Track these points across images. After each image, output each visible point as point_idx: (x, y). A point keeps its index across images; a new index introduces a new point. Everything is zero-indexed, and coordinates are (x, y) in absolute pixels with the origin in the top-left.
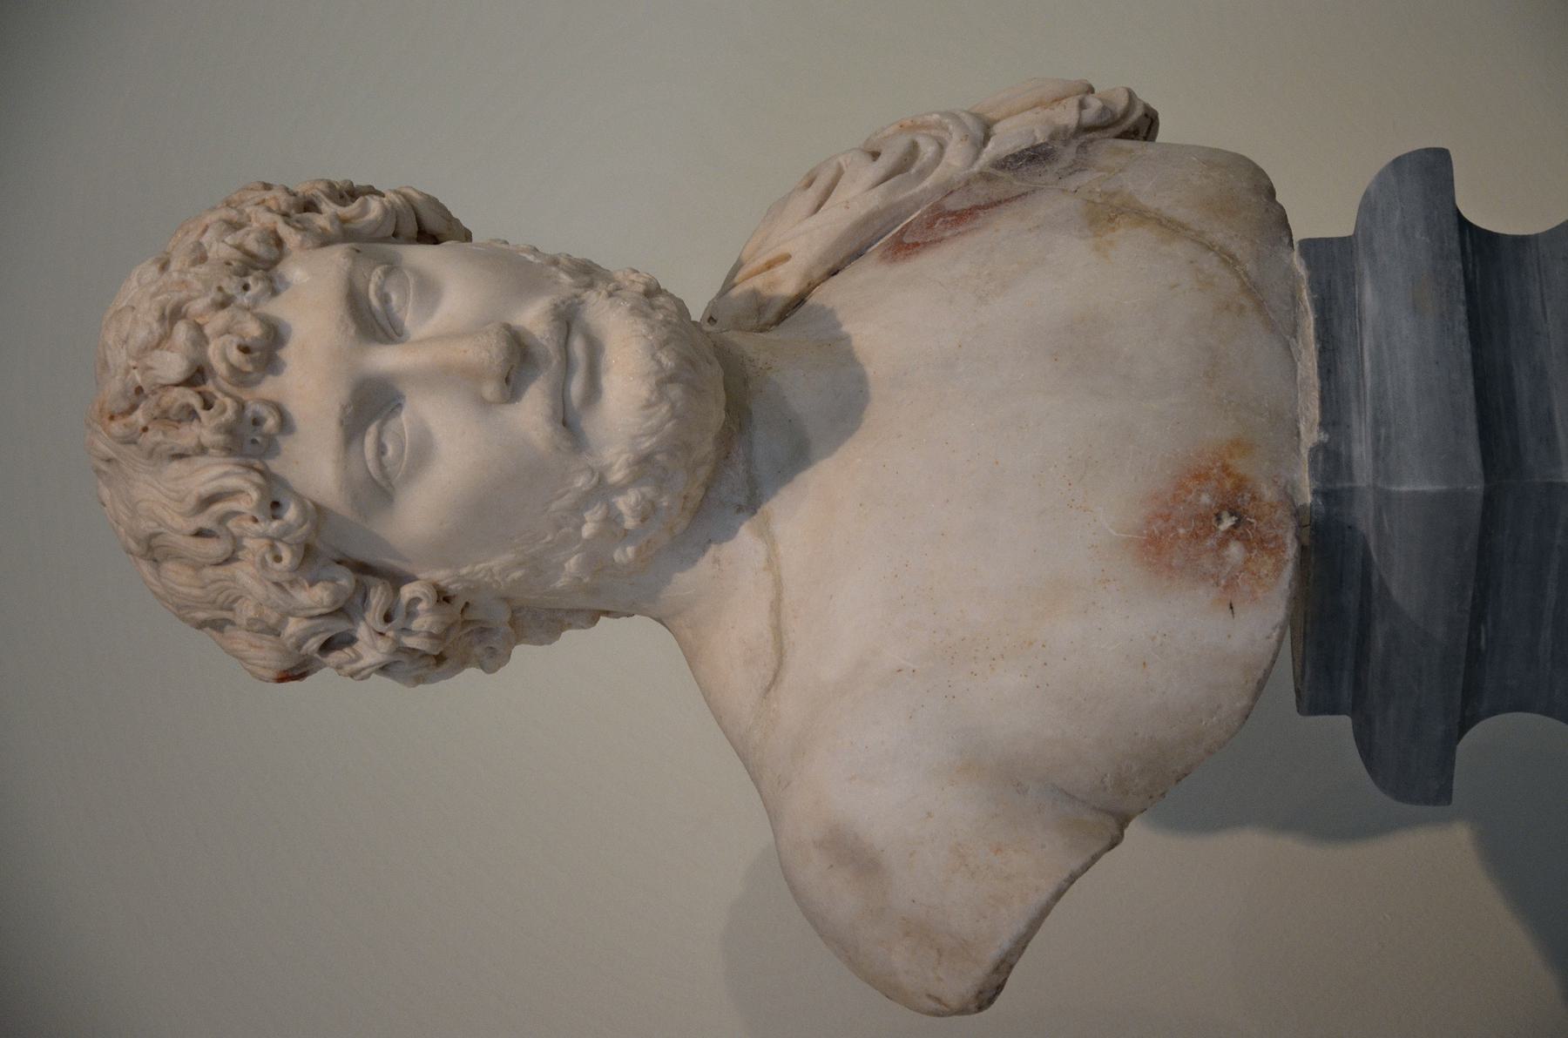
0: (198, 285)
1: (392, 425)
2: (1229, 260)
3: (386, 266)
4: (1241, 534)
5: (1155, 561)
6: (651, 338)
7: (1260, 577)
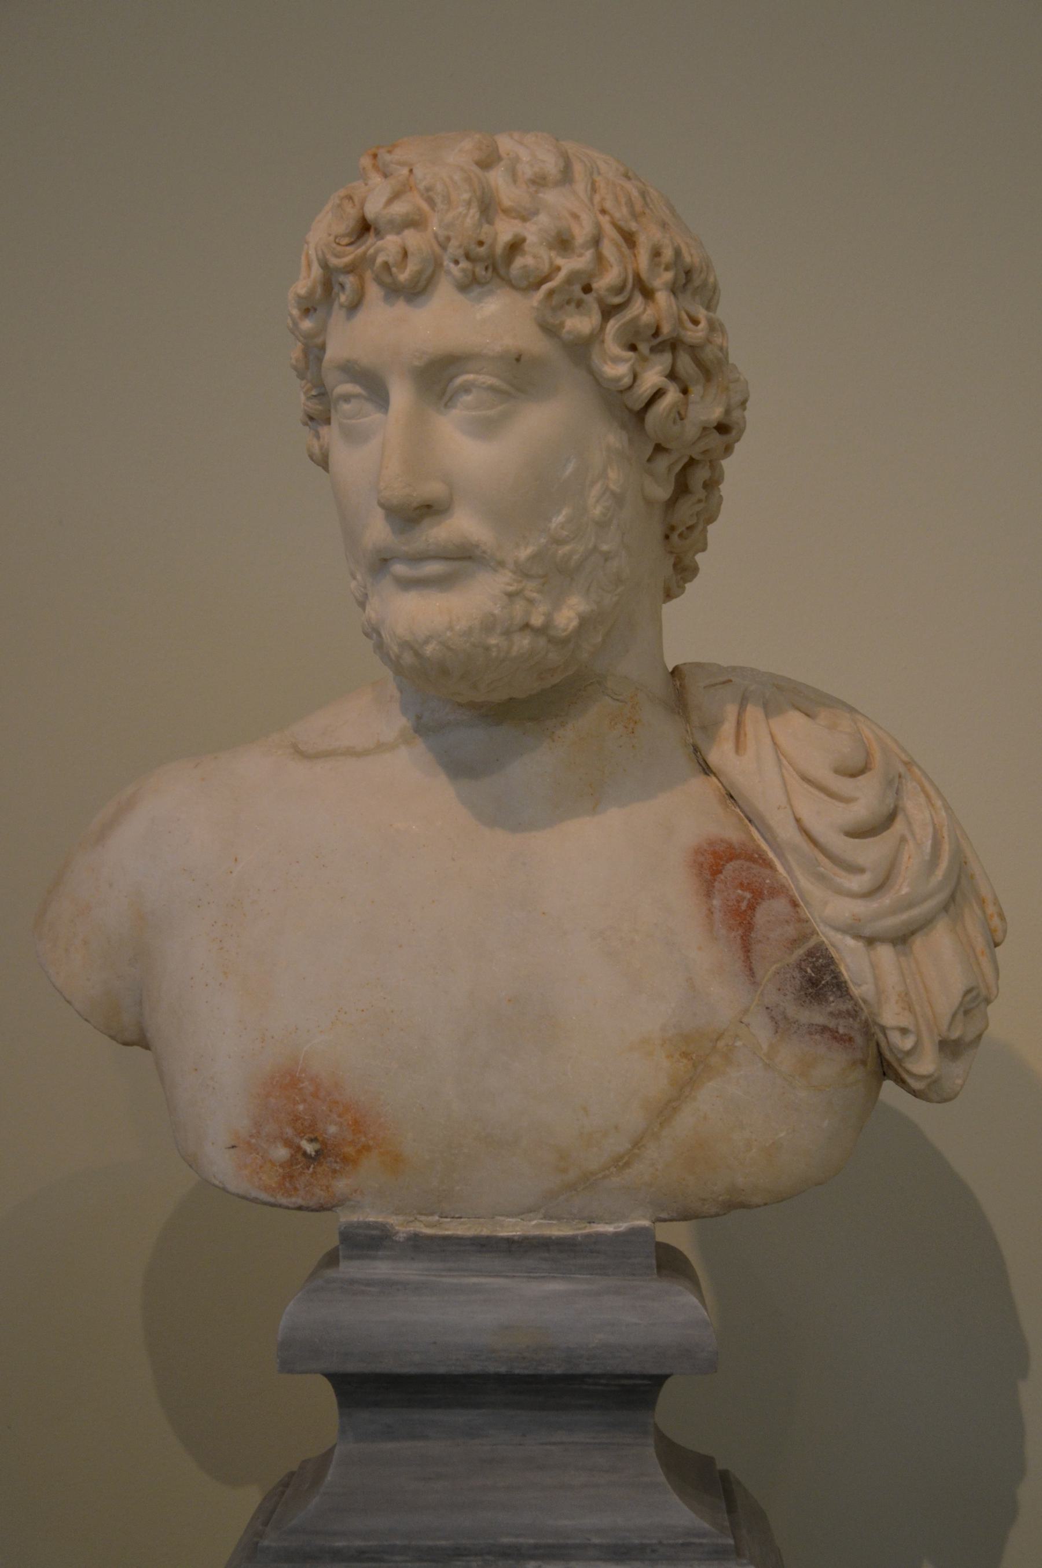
0: (449, 217)
1: (369, 407)
2: (621, 1162)
3: (505, 387)
4: (297, 1159)
5: (275, 1083)
6: (449, 634)
7: (258, 1173)
